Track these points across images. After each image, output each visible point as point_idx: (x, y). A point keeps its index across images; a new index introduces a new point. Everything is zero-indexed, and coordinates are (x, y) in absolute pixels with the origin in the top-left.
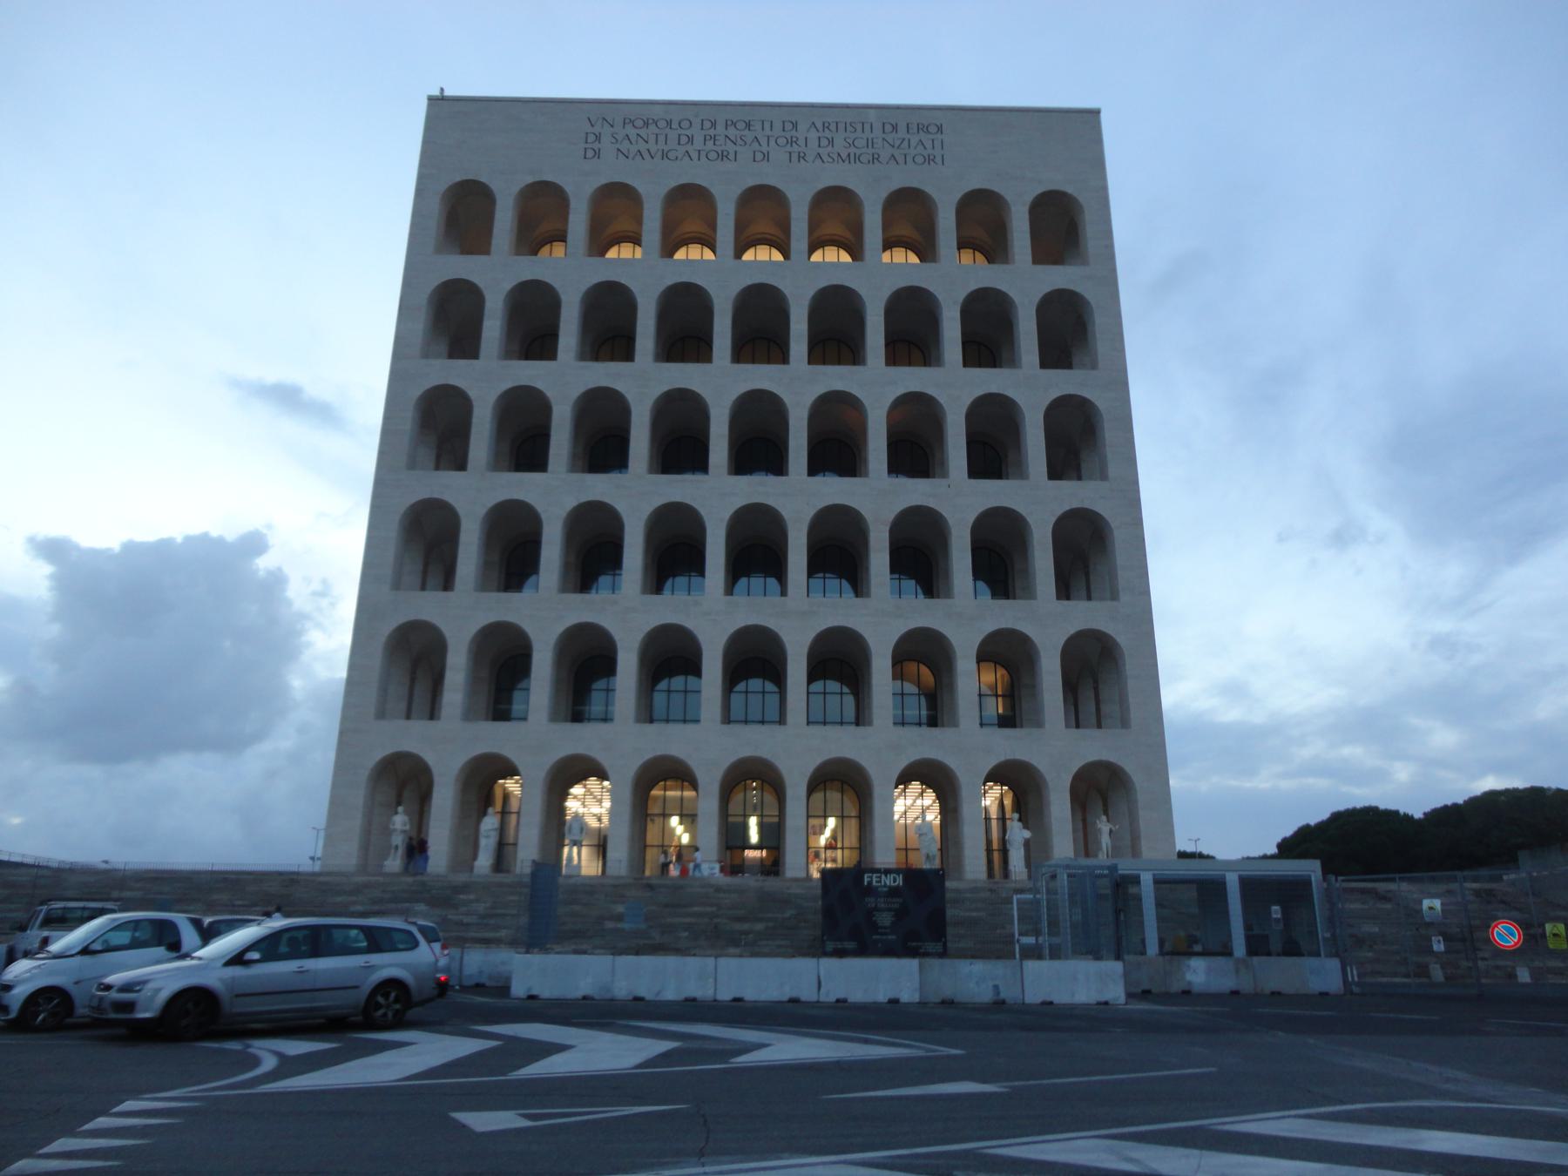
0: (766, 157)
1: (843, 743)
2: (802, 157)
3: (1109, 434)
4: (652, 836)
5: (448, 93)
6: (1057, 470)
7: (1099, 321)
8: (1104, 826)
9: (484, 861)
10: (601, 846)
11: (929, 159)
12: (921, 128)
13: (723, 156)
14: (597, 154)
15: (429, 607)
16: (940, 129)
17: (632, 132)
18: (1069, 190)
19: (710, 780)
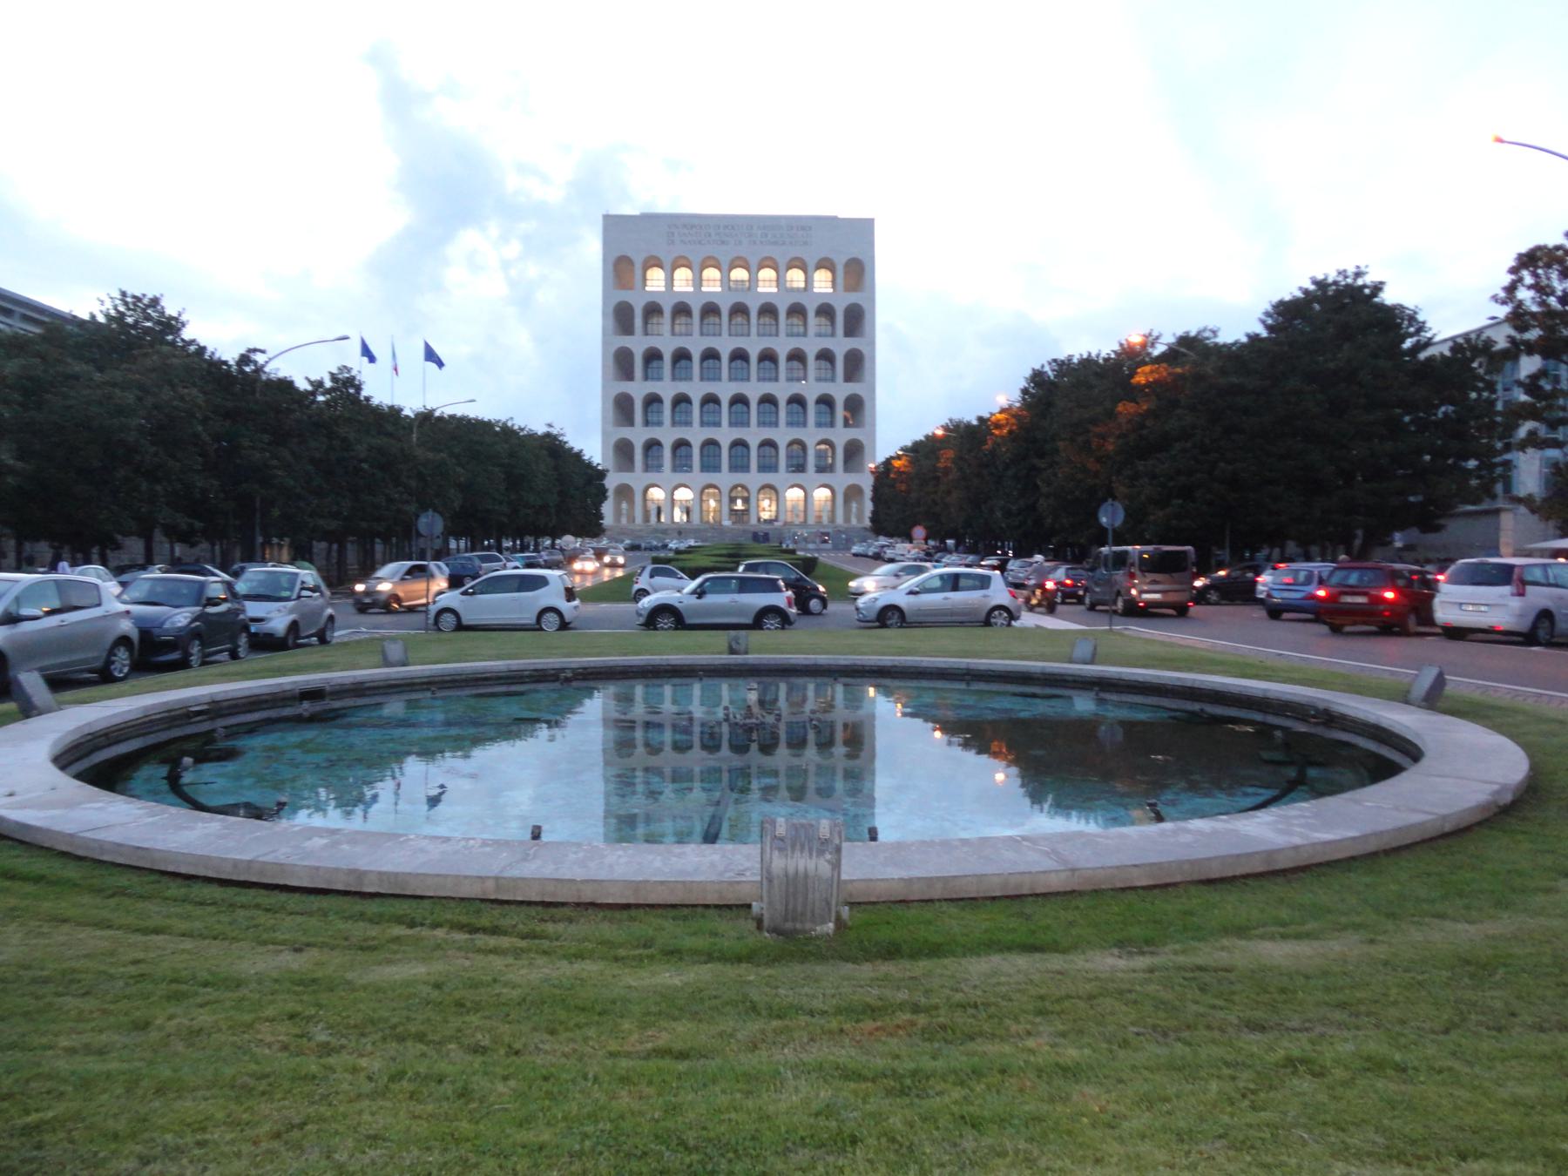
0: (740, 243)
1: (768, 478)
2: (755, 243)
3: (867, 364)
4: (704, 506)
5: (613, 212)
6: (849, 378)
7: (867, 316)
8: (854, 505)
9: (653, 519)
10: (688, 511)
11: (805, 243)
12: (803, 228)
13: (723, 242)
14: (673, 242)
15: (625, 433)
16: (810, 228)
17: (686, 231)
18: (860, 257)
19: (725, 491)
